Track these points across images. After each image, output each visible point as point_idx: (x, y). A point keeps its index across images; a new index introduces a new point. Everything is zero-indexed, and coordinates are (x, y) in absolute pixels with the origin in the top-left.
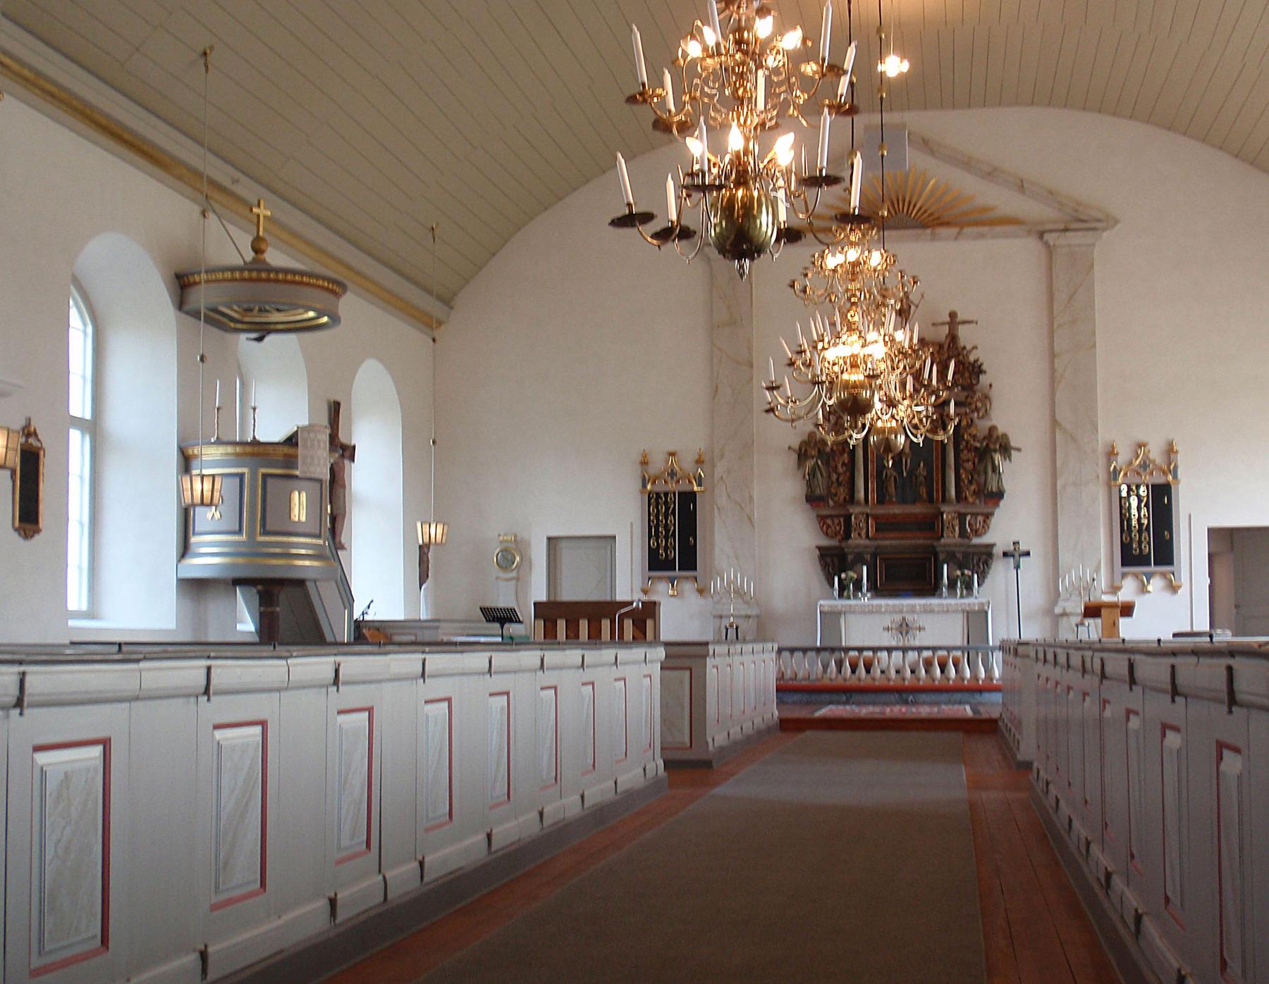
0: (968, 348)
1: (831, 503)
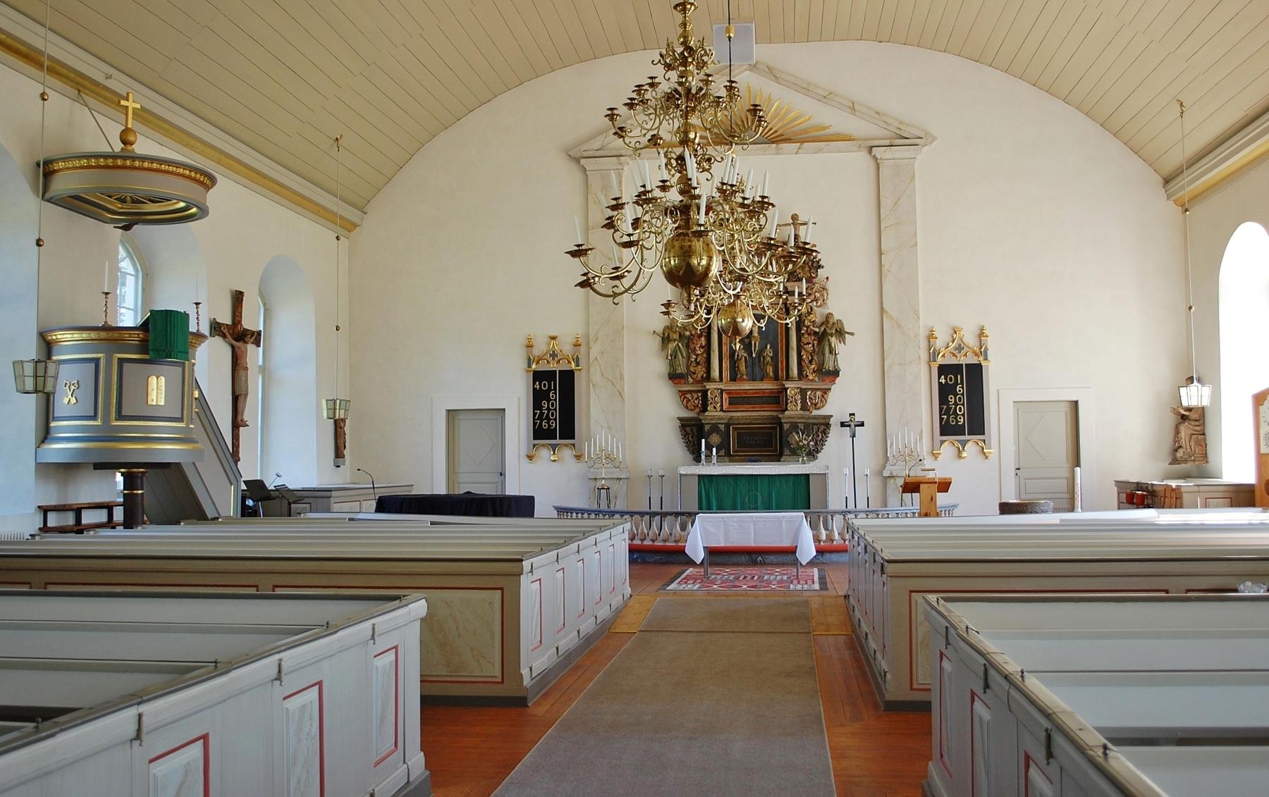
1: (691, 380)
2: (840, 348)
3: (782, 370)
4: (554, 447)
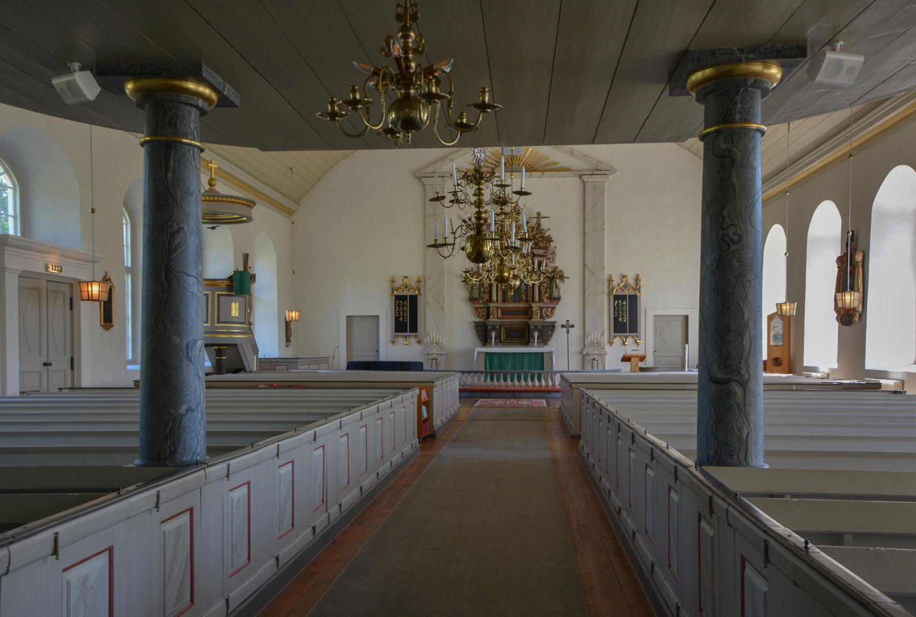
0: (546, 230)
1: (481, 301)
2: (561, 285)
3: (530, 297)
4: (406, 337)
